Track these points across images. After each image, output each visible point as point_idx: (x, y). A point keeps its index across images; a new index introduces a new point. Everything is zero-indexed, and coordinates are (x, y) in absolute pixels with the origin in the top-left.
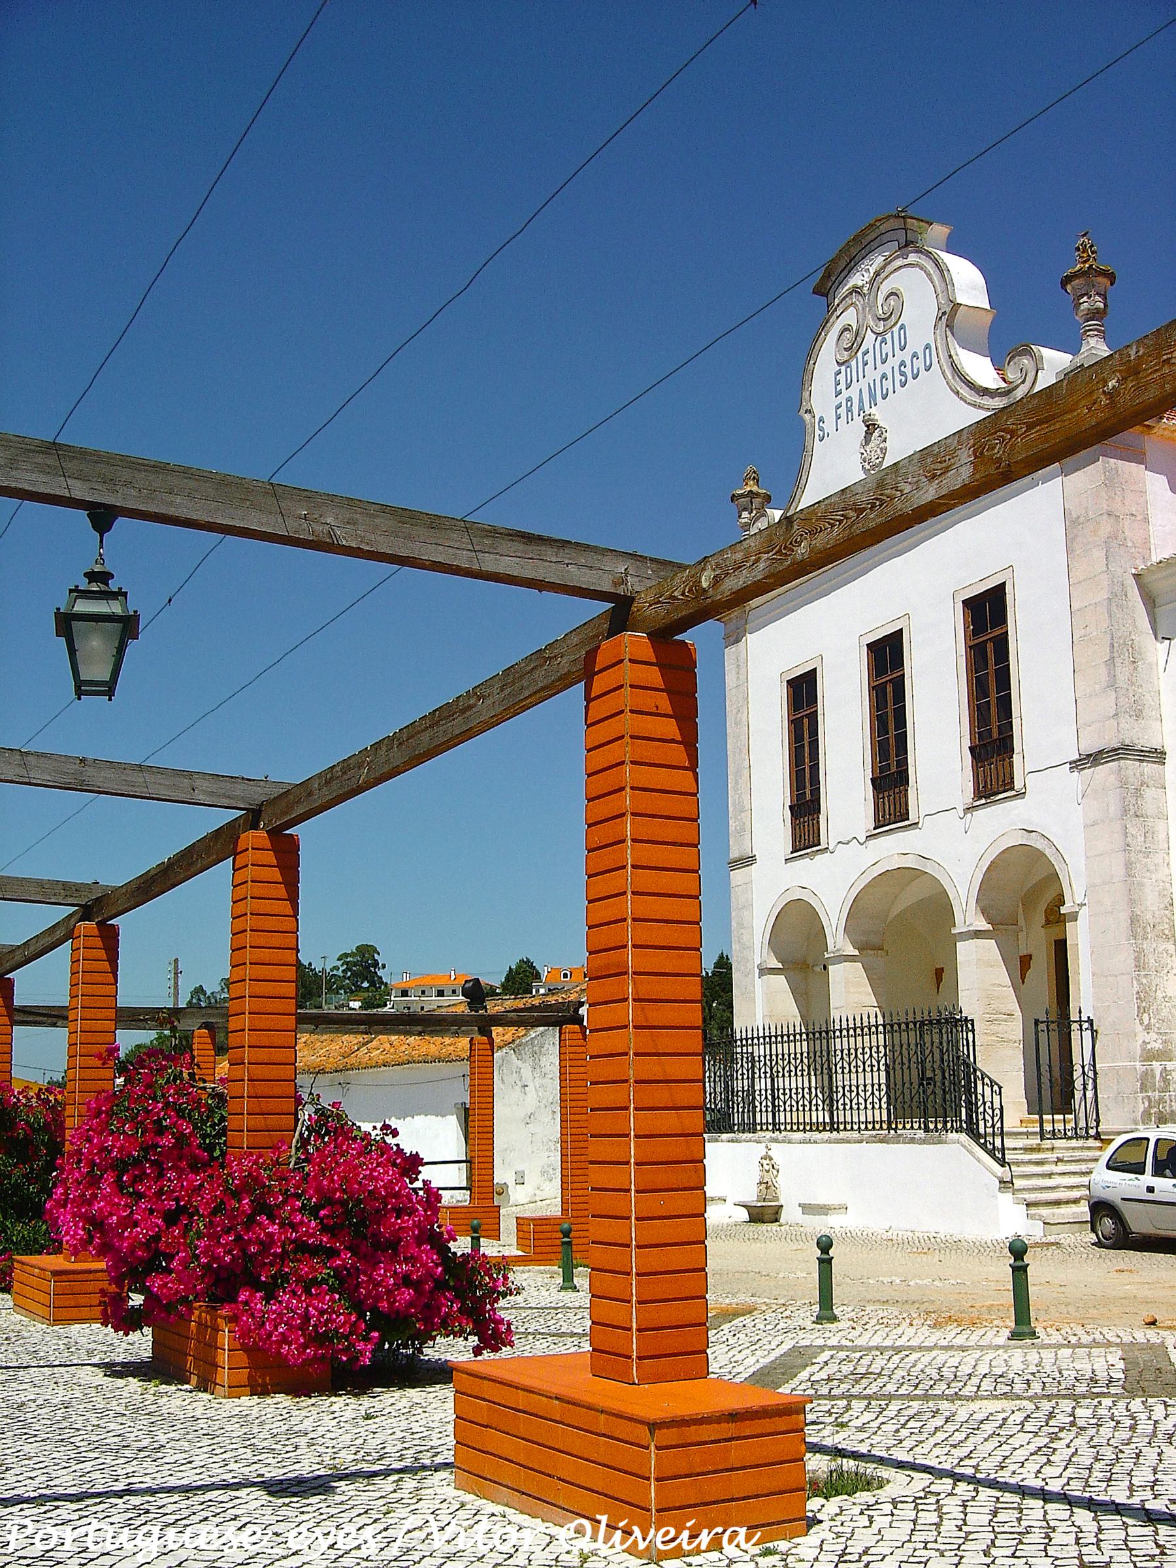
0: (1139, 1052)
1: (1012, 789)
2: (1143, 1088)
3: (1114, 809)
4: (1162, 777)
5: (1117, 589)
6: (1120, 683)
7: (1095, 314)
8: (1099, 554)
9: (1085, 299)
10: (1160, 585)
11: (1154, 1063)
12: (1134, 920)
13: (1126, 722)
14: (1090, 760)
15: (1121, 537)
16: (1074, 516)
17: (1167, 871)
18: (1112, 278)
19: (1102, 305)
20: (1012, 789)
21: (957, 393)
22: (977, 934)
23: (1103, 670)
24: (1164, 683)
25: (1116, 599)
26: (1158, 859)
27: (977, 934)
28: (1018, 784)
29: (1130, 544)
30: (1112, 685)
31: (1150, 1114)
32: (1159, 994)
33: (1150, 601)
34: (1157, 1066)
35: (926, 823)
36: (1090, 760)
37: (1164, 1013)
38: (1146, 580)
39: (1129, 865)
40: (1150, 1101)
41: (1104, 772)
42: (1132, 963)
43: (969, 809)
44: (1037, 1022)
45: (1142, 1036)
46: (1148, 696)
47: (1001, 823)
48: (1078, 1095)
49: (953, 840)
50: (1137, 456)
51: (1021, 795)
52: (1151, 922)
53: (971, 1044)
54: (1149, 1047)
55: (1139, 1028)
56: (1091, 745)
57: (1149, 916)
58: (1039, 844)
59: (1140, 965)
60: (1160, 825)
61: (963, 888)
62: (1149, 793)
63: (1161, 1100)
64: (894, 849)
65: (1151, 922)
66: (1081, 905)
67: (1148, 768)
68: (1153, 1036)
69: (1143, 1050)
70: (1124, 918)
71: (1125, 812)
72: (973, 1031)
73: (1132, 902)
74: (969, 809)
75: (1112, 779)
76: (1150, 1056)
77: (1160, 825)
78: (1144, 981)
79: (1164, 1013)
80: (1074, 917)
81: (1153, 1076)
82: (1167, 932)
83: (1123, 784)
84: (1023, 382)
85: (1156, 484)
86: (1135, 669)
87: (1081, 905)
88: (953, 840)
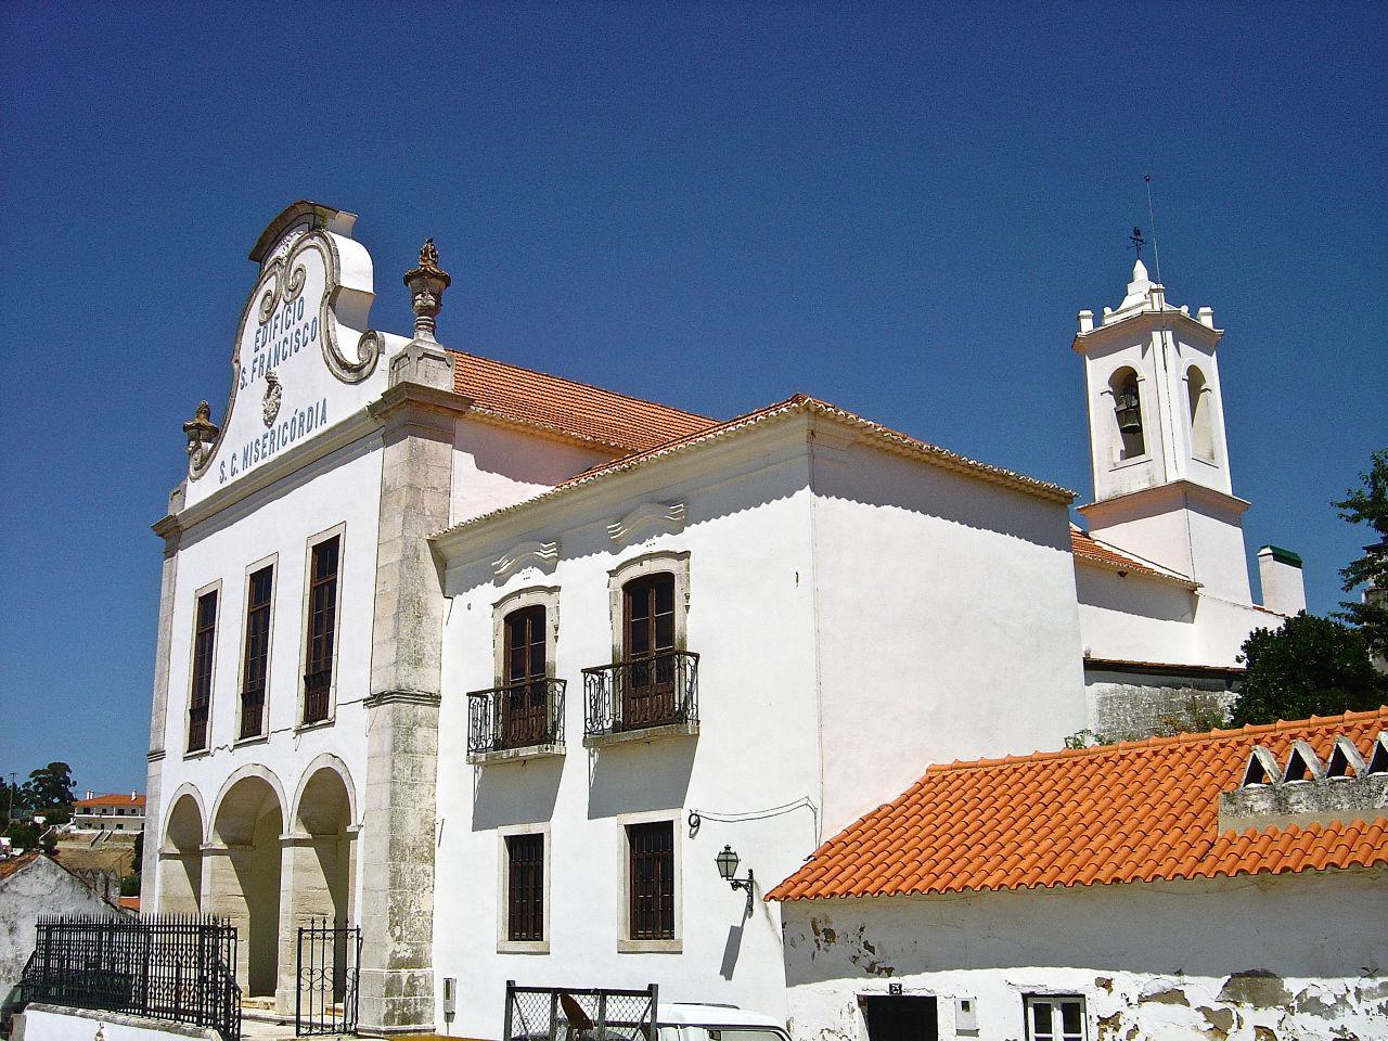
0: (388, 961)
1: (326, 718)
2: (389, 993)
3: (387, 746)
4: (435, 718)
5: (410, 552)
6: (402, 636)
7: (425, 310)
8: (399, 520)
9: (419, 296)
10: (450, 549)
11: (402, 970)
12: (394, 845)
13: (404, 670)
14: (376, 699)
15: (419, 506)
16: (388, 484)
17: (431, 801)
18: (447, 281)
19: (434, 304)
20: (326, 718)
21: (328, 364)
22: (297, 842)
23: (391, 622)
24: (448, 635)
25: (409, 560)
26: (424, 790)
27: (297, 842)
28: (330, 715)
29: (428, 513)
30: (396, 636)
31: (394, 1016)
32: (413, 909)
33: (442, 563)
34: (404, 973)
35: (273, 738)
36: (376, 699)
37: (418, 926)
38: (440, 545)
39: (394, 795)
40: (394, 1005)
41: (384, 710)
42: (388, 882)
43: (299, 731)
44: (301, 931)
45: (392, 946)
46: (429, 647)
47: (319, 743)
48: (348, 994)
49: (287, 760)
50: (446, 436)
51: (332, 724)
52: (411, 845)
53: (232, 955)
54: (399, 956)
55: (389, 939)
56: (378, 688)
57: (409, 841)
58: (339, 769)
59: (395, 882)
60: (429, 761)
61: (289, 798)
62: (421, 733)
63: (406, 1003)
64: (250, 760)
65: (411, 845)
66: (360, 826)
67: (422, 710)
68: (404, 946)
69: (392, 958)
70: (386, 840)
71: (395, 749)
72: (236, 938)
73: (393, 828)
74: (299, 731)
75: (389, 719)
76: (397, 963)
77: (429, 761)
78: (399, 898)
79: (418, 926)
80: (355, 836)
81: (400, 982)
82: (426, 854)
83: (397, 723)
84: (369, 363)
85: (464, 462)
86: (420, 623)
87: (360, 826)
88: (287, 760)
